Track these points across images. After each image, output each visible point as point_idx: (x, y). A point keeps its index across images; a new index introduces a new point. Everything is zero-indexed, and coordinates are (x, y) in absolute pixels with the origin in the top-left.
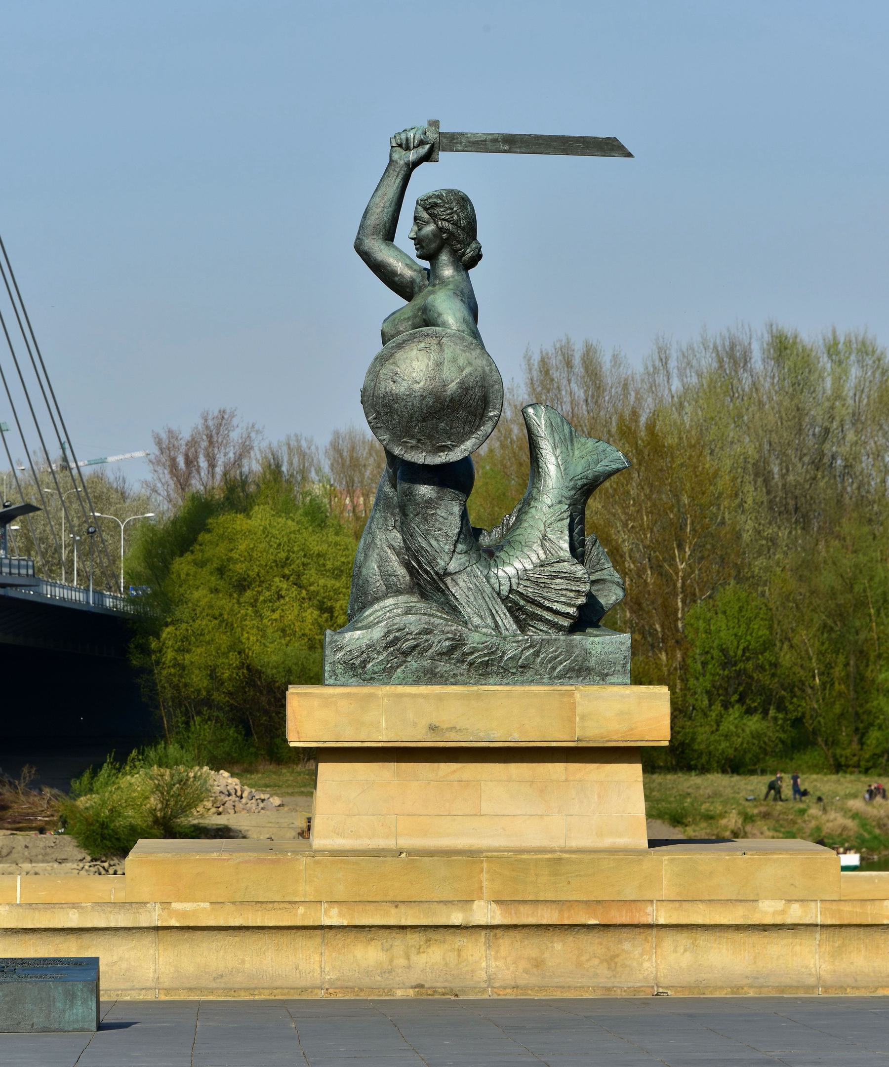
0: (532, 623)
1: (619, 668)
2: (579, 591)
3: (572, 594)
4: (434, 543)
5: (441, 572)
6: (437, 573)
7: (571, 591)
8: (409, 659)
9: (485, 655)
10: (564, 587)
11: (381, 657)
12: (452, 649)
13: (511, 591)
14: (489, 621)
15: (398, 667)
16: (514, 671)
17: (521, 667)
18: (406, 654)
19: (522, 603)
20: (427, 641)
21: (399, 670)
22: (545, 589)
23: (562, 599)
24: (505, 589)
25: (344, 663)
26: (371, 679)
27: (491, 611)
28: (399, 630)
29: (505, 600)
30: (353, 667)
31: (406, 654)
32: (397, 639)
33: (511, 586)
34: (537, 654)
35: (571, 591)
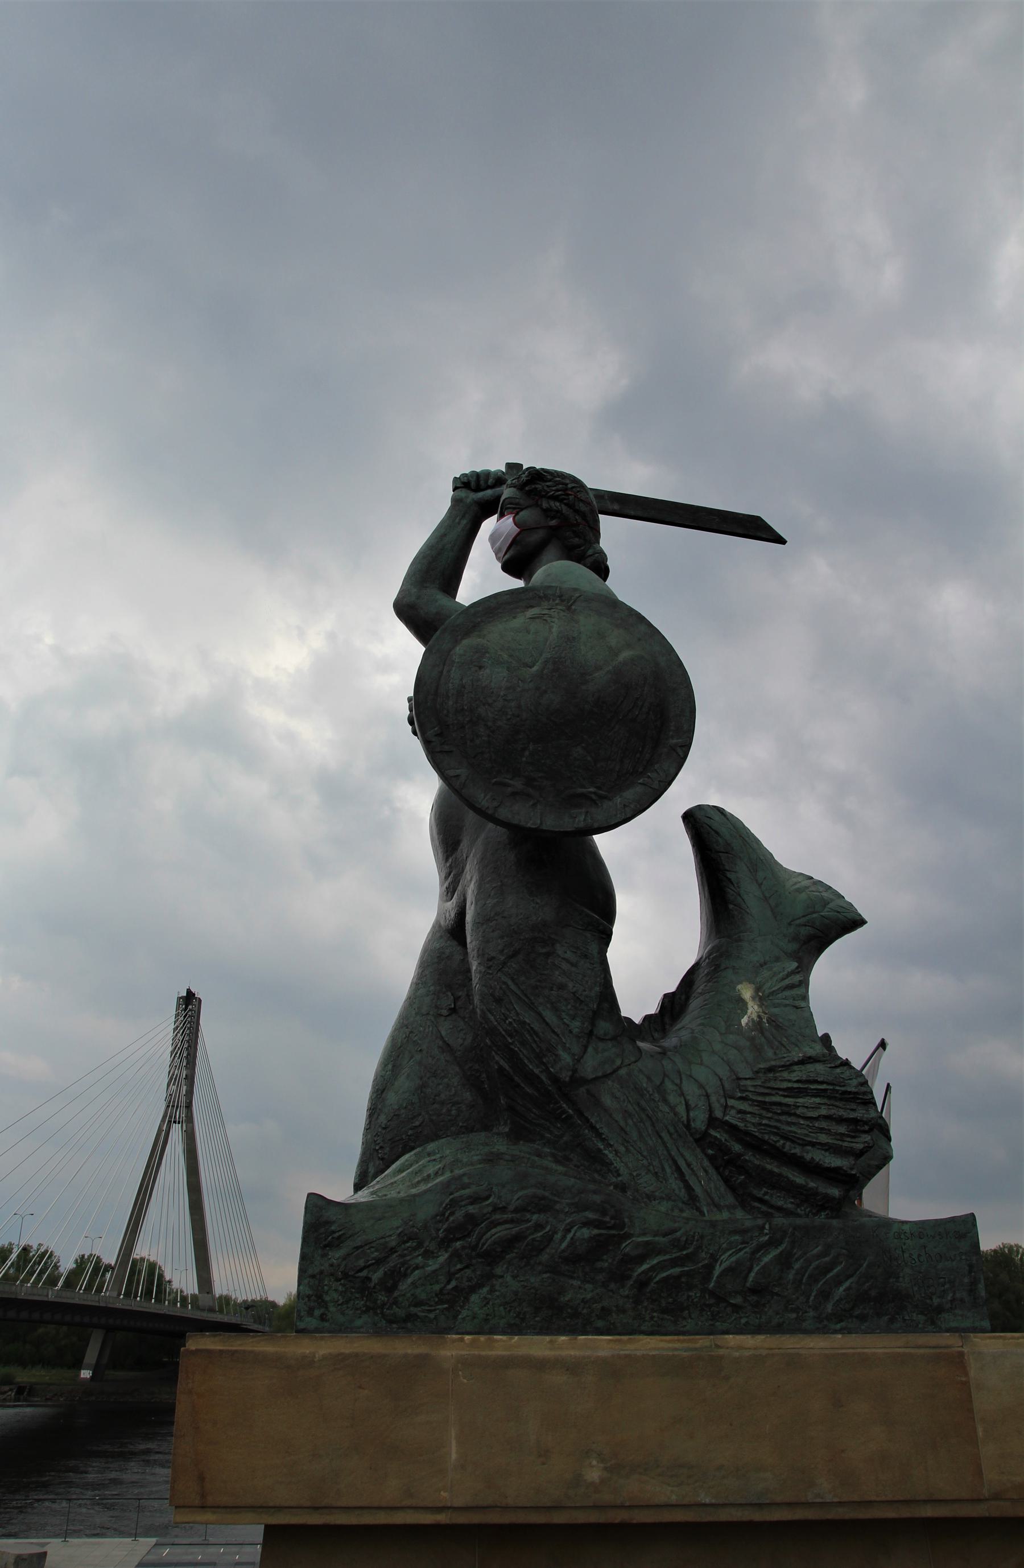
0: (759, 1193)
2: (855, 1121)
3: (842, 1129)
4: (549, 1015)
5: (565, 1076)
6: (555, 1080)
7: (841, 1120)
8: (498, 1270)
9: (674, 1263)
10: (824, 1111)
11: (433, 1265)
12: (599, 1246)
13: (713, 1121)
14: (674, 1184)
15: (473, 1289)
16: (738, 1300)
17: (753, 1291)
18: (492, 1257)
19: (737, 1148)
20: (539, 1226)
21: (474, 1298)
22: (783, 1118)
23: (823, 1138)
24: (700, 1119)
25: (346, 1275)
26: (409, 1317)
27: (675, 1162)
28: (475, 1200)
29: (702, 1140)
31: (492, 1257)
32: (472, 1220)
33: (711, 1110)
34: (785, 1261)
35: (841, 1120)
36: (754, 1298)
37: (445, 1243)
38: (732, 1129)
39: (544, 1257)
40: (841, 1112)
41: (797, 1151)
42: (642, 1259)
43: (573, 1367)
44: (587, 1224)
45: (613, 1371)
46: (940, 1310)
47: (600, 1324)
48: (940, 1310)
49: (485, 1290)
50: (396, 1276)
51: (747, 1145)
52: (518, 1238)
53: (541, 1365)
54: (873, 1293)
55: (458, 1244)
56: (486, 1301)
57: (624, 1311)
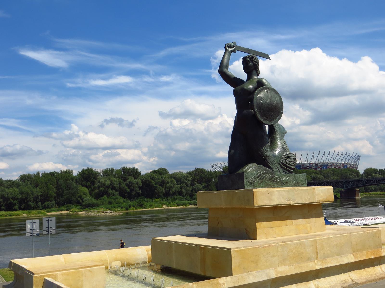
1: (304, 182)
5: (265, 156)
6: (264, 157)
12: (272, 177)
15: (261, 183)
18: (262, 179)
21: (261, 184)
26: (256, 187)
29: (279, 164)
30: (251, 183)
32: (260, 175)
34: (289, 179)
36: (286, 183)
37: (258, 178)
38: (282, 163)
39: (267, 179)
40: (293, 161)
41: (289, 165)
42: (276, 179)
43: (284, 191)
44: (271, 175)
45: (288, 191)
46: (303, 184)
47: (273, 187)
48: (303, 184)
49: (262, 183)
50: (254, 182)
51: (283, 165)
52: (264, 177)
53: (281, 191)
54: (297, 182)
55: (259, 178)
56: (262, 184)
57: (274, 185)
